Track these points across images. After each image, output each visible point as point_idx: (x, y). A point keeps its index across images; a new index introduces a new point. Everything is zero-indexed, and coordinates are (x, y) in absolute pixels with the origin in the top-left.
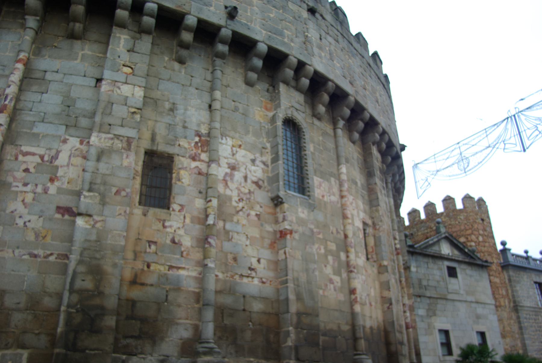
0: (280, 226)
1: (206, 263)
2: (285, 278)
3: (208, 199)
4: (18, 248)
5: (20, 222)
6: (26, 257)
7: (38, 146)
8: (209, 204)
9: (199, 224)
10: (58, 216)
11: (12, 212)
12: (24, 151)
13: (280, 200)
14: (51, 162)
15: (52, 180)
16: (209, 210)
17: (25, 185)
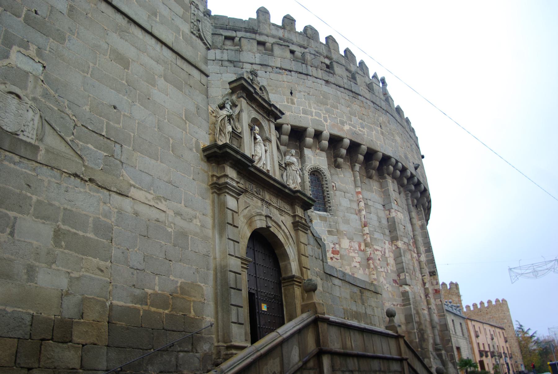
0: (434, 287)
1: (430, 307)
2: (443, 314)
3: (424, 274)
4: (389, 301)
5: (385, 287)
6: (392, 306)
7: (378, 246)
8: (424, 277)
9: (427, 288)
10: (394, 284)
11: (382, 282)
12: (376, 248)
13: (434, 273)
14: (385, 255)
15: (388, 265)
16: (425, 281)
17: (381, 268)
